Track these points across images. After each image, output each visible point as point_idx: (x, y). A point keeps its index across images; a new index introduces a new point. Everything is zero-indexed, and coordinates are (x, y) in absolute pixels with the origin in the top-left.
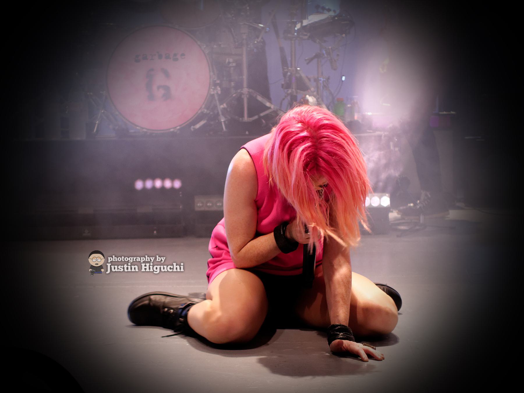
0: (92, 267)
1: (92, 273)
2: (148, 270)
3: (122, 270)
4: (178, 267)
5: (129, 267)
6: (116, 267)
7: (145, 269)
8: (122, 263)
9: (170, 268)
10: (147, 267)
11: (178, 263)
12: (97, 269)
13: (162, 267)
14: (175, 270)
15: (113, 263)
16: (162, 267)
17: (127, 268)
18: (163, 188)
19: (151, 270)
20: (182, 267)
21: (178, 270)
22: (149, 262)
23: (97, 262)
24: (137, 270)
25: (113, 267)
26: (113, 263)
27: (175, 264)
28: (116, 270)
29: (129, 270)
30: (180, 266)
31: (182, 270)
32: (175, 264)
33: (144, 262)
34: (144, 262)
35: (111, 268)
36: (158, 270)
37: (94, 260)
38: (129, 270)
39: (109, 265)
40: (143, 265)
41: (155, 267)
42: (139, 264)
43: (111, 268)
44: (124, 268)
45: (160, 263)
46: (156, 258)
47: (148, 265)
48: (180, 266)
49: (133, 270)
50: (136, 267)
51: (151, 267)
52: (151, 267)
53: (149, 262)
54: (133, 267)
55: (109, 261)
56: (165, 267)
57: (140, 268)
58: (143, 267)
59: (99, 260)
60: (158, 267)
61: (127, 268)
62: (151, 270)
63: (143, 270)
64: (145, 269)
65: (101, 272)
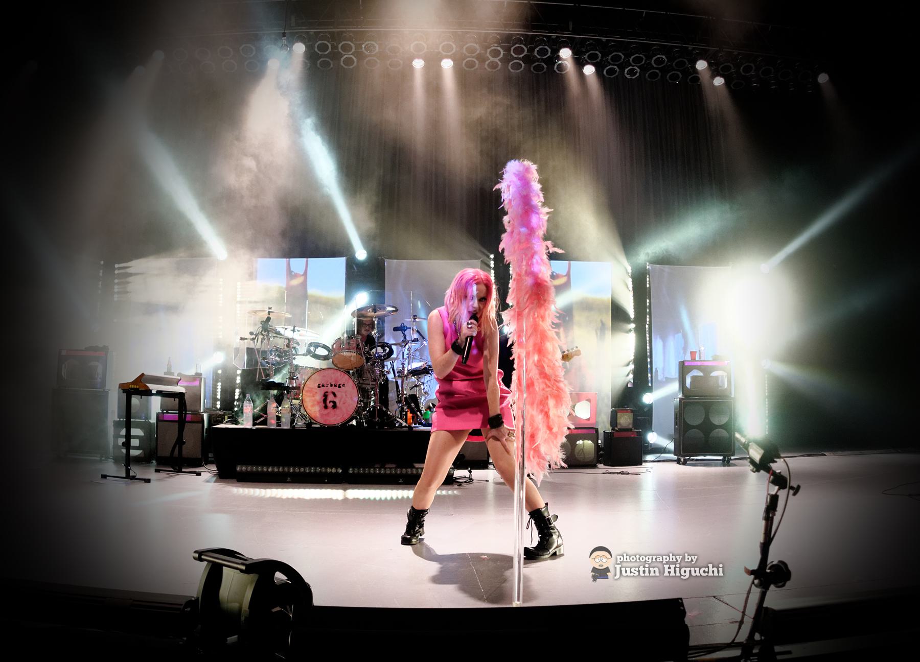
0: (594, 570)
1: (595, 578)
2: (672, 574)
3: (637, 574)
4: (715, 570)
5: (647, 570)
6: (628, 570)
7: (669, 572)
8: (636, 564)
9: (704, 572)
10: (672, 570)
11: (716, 564)
12: (600, 573)
13: (693, 570)
14: (711, 574)
15: (624, 564)
16: (693, 570)
17: (644, 572)
18: (316, 467)
19: (678, 574)
20: (721, 570)
21: (716, 574)
22: (675, 563)
23: (601, 563)
24: (657, 574)
25: (623, 570)
26: (624, 564)
27: (710, 566)
28: (628, 573)
29: (647, 574)
30: (718, 567)
31: (721, 574)
32: (710, 566)
33: (667, 563)
34: (667, 563)
35: (621, 571)
36: (687, 574)
37: (597, 560)
38: (647, 574)
39: (618, 567)
40: (666, 566)
41: (683, 570)
42: (660, 565)
43: (621, 571)
44: (639, 571)
45: (690, 565)
46: (684, 558)
47: (673, 566)
48: (718, 567)
49: (652, 574)
50: (657, 570)
51: (678, 570)
52: (678, 570)
53: (675, 563)
54: (652, 570)
55: (619, 561)
56: (697, 569)
57: (662, 572)
58: (667, 570)
59: (605, 560)
60: (688, 570)
61: (644, 572)
62: (678, 574)
63: (666, 574)
64: (669, 572)
65: (607, 577)
